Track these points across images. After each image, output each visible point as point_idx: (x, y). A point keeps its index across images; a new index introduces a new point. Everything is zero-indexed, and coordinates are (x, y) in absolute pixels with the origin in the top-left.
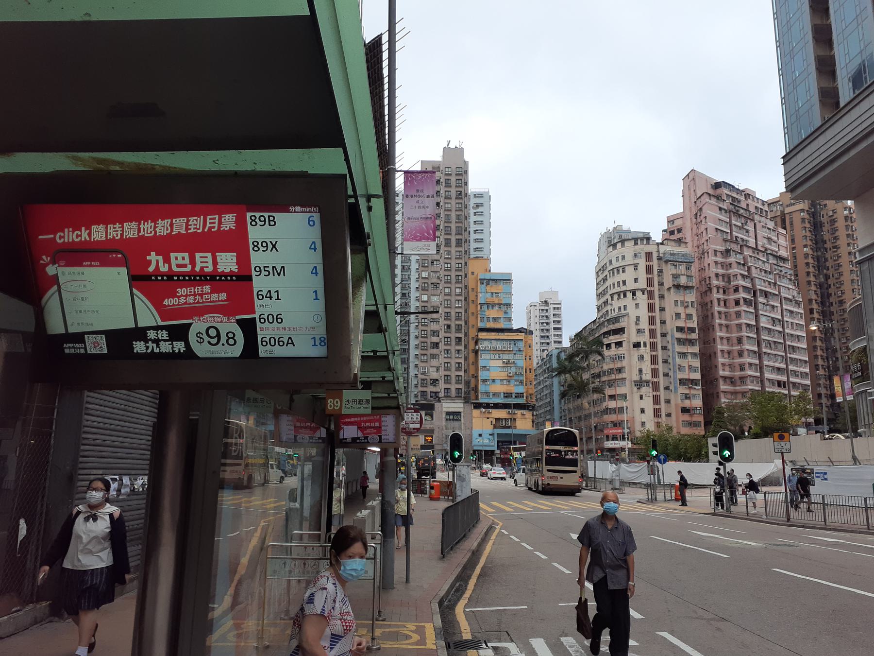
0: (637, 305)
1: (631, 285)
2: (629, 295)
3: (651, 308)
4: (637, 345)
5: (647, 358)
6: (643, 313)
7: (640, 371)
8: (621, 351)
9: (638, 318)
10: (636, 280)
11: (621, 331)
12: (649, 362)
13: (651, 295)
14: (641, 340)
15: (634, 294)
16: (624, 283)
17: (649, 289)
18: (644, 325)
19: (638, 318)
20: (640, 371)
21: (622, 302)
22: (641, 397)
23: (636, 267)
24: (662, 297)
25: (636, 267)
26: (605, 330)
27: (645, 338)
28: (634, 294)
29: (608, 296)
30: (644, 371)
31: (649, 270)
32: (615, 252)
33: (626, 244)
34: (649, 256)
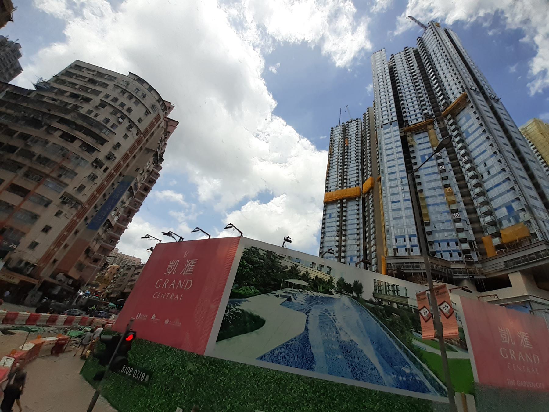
0: (126, 136)
1: (134, 116)
2: (126, 123)
3: (132, 149)
4: (98, 164)
5: (98, 182)
6: (126, 145)
7: (81, 188)
8: (85, 155)
9: (118, 145)
10: (140, 120)
11: (103, 141)
12: (95, 187)
13: (138, 142)
14: (107, 164)
15: (130, 127)
16: (129, 110)
17: (142, 135)
18: (119, 155)
19: (118, 145)
20: (81, 188)
21: (113, 120)
22: (58, 214)
23: (147, 113)
24: (141, 148)
25: (147, 113)
26: (68, 117)
27: (111, 165)
28: (130, 127)
29: (96, 100)
30: (85, 191)
31: (152, 125)
32: (138, 85)
33: (152, 92)
34: (158, 118)
